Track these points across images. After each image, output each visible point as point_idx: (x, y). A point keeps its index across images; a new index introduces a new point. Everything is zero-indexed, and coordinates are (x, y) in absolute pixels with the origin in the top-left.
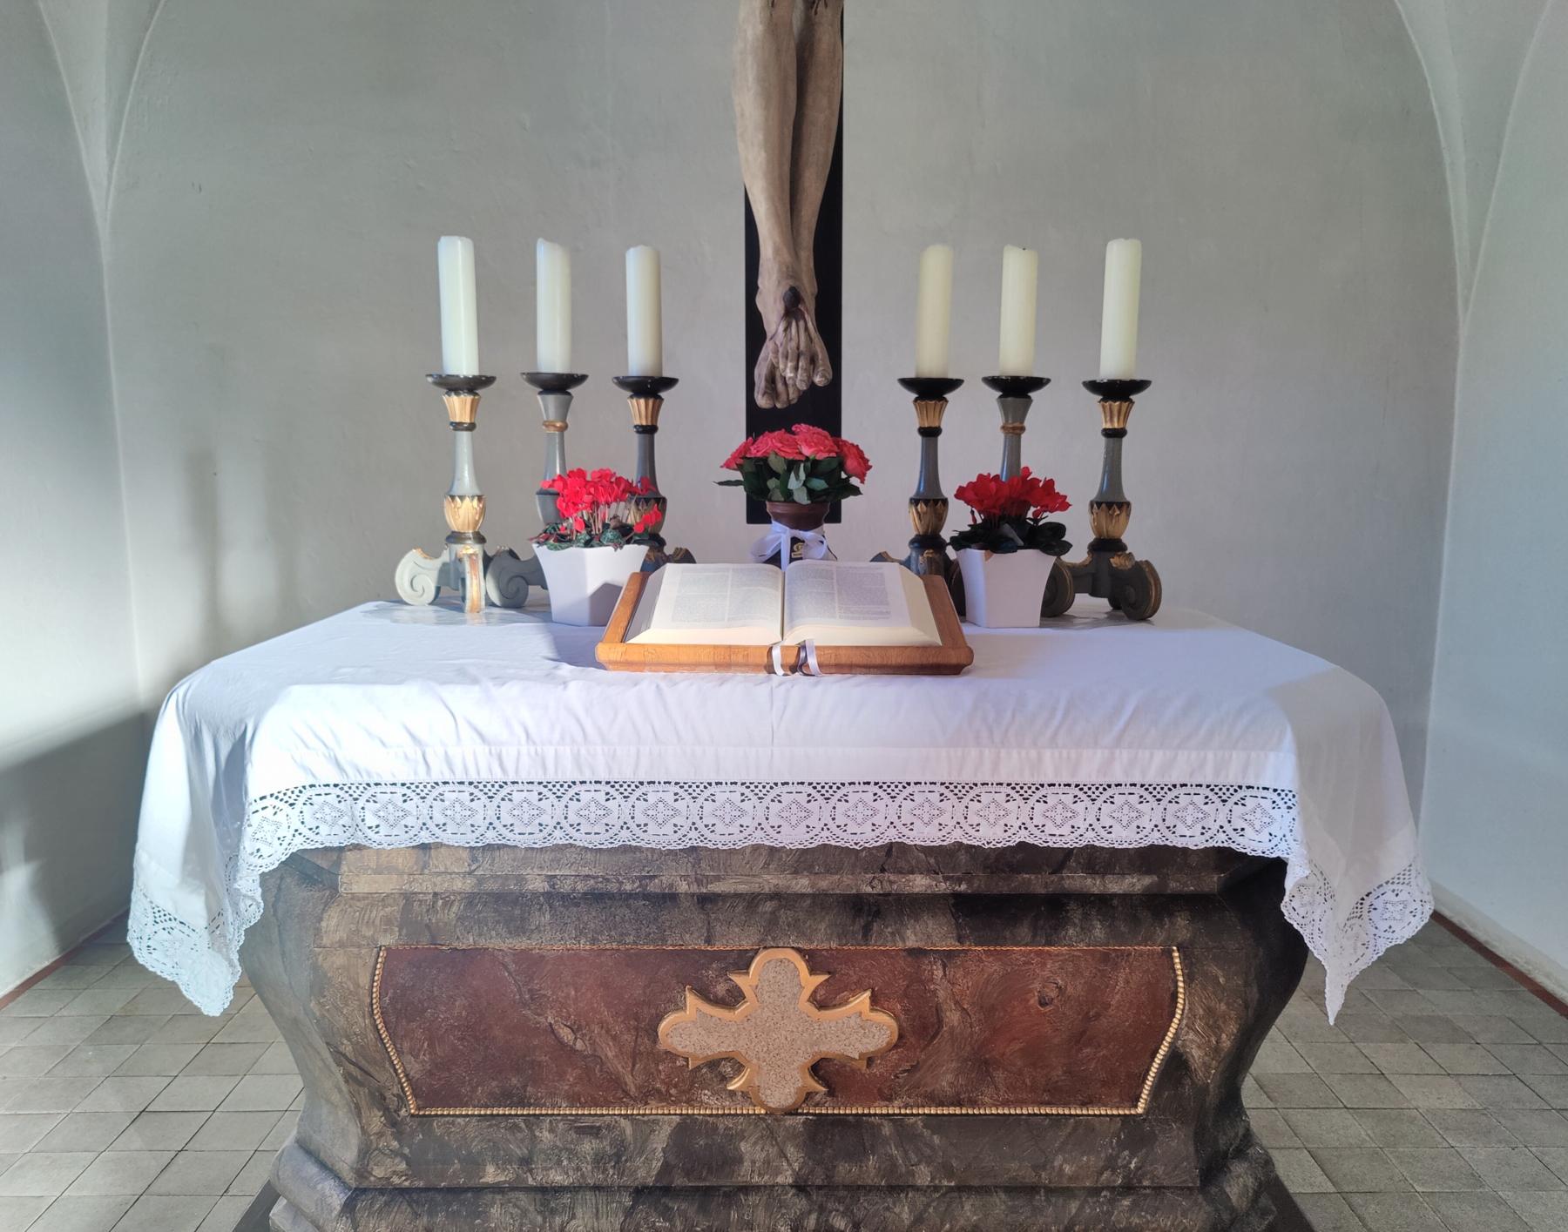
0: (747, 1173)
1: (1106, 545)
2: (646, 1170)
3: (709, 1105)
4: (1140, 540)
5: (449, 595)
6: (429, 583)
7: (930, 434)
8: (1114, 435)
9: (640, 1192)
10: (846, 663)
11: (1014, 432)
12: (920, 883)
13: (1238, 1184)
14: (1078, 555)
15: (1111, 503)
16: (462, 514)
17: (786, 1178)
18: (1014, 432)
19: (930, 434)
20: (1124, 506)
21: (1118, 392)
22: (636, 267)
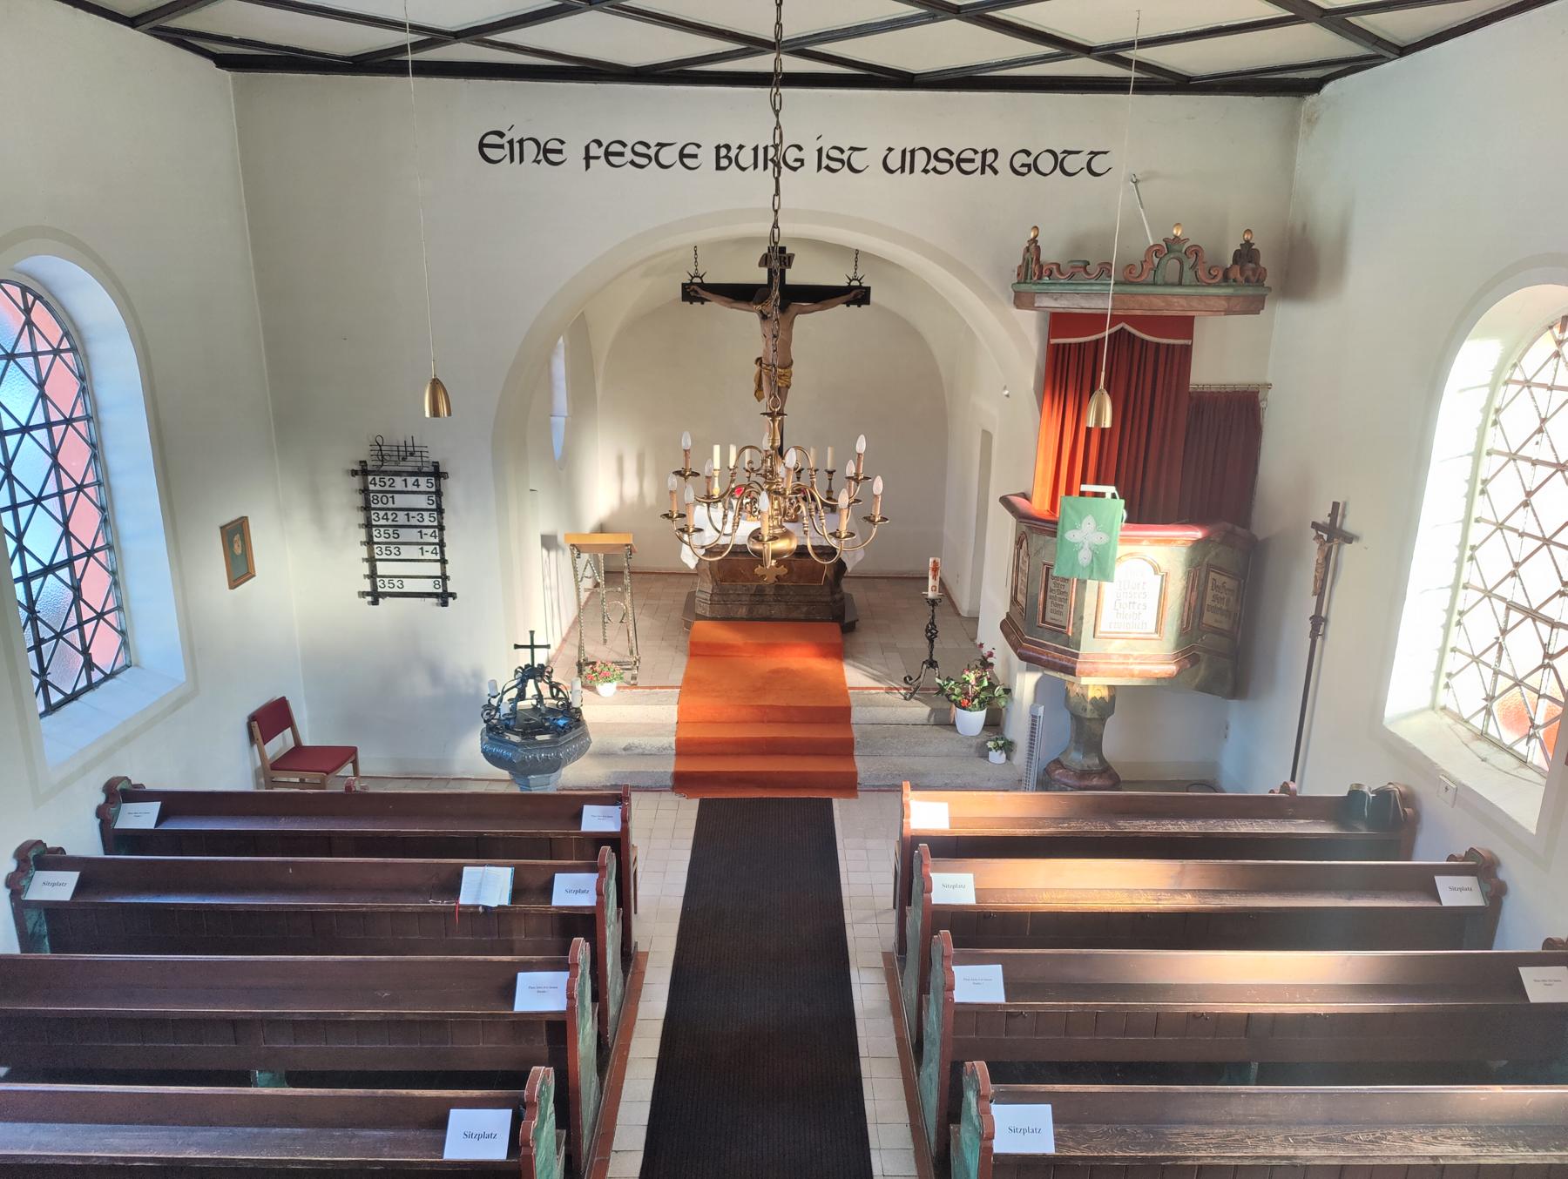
0: (766, 593)
2: (753, 592)
8: (830, 479)
9: (751, 595)
13: (837, 596)
17: (771, 593)
20: (832, 492)
21: (831, 473)
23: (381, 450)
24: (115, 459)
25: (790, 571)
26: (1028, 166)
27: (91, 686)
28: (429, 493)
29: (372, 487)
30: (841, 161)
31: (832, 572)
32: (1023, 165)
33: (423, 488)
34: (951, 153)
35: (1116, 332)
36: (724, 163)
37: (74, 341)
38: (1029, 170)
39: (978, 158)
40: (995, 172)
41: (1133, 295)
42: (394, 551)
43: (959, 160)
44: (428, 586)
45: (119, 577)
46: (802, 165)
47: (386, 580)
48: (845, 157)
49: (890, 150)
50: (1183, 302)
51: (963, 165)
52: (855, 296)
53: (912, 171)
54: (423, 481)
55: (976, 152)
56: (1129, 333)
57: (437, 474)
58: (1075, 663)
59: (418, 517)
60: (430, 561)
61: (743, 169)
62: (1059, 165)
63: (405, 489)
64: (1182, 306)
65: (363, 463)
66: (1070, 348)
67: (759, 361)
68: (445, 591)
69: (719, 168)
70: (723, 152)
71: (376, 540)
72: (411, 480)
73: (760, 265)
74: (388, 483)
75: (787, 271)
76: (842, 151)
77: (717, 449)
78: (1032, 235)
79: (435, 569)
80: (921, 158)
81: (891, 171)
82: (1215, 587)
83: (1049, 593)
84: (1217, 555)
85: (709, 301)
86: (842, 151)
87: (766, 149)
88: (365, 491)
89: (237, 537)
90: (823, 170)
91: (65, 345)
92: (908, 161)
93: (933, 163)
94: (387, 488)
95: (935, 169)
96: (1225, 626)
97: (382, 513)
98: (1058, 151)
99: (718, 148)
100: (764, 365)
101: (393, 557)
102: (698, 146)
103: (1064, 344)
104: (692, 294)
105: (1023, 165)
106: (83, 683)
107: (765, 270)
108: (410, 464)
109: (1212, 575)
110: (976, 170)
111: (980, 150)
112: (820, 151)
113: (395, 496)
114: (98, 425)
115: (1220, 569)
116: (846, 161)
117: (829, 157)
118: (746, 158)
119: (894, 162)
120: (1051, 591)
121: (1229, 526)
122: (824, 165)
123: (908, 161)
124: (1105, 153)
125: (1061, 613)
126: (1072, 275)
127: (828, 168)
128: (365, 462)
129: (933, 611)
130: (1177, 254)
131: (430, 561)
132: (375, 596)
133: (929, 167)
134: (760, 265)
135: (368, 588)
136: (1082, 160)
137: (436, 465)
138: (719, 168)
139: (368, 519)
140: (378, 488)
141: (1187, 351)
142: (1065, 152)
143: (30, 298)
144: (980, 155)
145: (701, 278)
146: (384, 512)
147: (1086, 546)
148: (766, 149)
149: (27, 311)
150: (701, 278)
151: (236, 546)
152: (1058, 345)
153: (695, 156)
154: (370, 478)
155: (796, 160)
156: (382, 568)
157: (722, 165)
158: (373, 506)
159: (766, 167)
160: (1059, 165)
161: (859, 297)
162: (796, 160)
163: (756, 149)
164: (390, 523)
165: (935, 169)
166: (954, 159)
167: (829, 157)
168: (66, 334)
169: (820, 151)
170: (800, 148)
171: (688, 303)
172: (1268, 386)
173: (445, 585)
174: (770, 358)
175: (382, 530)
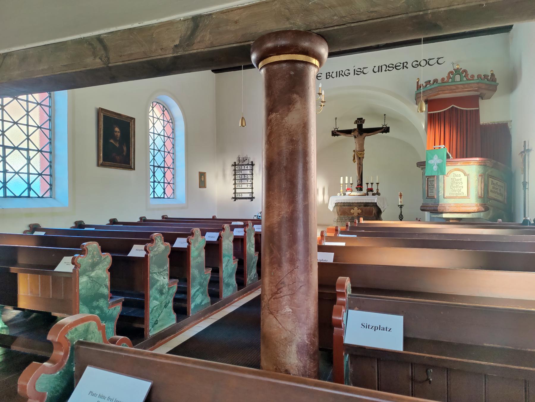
1: (377, 192)
2: (350, 219)
3: (353, 216)
4: (379, 192)
5: (341, 195)
6: (339, 195)
7: (367, 186)
8: (378, 186)
10: (359, 195)
11: (372, 186)
12: (362, 205)
14: (375, 192)
15: (378, 190)
16: (341, 190)
18: (372, 186)
19: (367, 186)
20: (378, 190)
21: (378, 184)
22: (351, 178)
23: (239, 159)
24: (177, 148)
25: (362, 211)
26: (418, 65)
27: (164, 198)
28: (250, 170)
29: (236, 169)
30: (361, 72)
31: (376, 212)
32: (416, 65)
33: (249, 168)
34: (393, 65)
35: (451, 108)
36: (328, 77)
37: (172, 121)
38: (418, 66)
39: (402, 65)
40: (407, 68)
41: (444, 86)
42: (241, 186)
43: (396, 66)
44: (248, 195)
45: (174, 176)
46: (350, 74)
47: (238, 194)
48: (362, 71)
49: (375, 67)
50: (462, 86)
51: (397, 68)
52: (384, 130)
53: (381, 71)
54: (249, 166)
55: (401, 63)
56: (456, 108)
57: (253, 165)
58: (437, 207)
59: (247, 176)
60: (249, 188)
61: (333, 78)
62: (427, 63)
63: (244, 169)
64: (462, 88)
65: (235, 163)
66: (433, 115)
67: (354, 151)
68: (252, 197)
69: (327, 78)
70: (328, 74)
71: (236, 183)
72: (246, 166)
73: (354, 123)
74: (240, 168)
75: (363, 124)
76: (361, 69)
77: (342, 178)
78: (417, 81)
79: (250, 191)
80: (384, 68)
81: (375, 72)
82: (493, 183)
83: (429, 187)
84: (491, 172)
85: (340, 135)
86: (361, 69)
87: (339, 72)
88: (235, 170)
89: (203, 176)
90: (356, 75)
91: (170, 121)
92: (380, 69)
93: (388, 68)
94: (240, 169)
95: (388, 70)
96: (500, 198)
97: (238, 176)
98: (427, 60)
99: (327, 74)
100: (355, 152)
101: (240, 187)
102: (321, 74)
103: (433, 113)
104: (334, 133)
105: (416, 65)
106: (162, 196)
107: (356, 125)
108: (246, 163)
109: (490, 179)
110: (400, 69)
111: (402, 63)
112: (355, 70)
113: (242, 171)
114: (175, 140)
115: (493, 177)
116: (362, 71)
117: (357, 71)
118: (334, 75)
119: (376, 70)
120: (429, 186)
121: (495, 161)
122: (356, 73)
123: (380, 69)
124: (443, 58)
125: (433, 192)
126: (426, 85)
127: (357, 74)
128: (235, 162)
129: (401, 210)
130: (458, 73)
131: (249, 188)
132: (235, 199)
133: (387, 70)
134: (354, 123)
135: (234, 197)
136: (435, 60)
137: (252, 162)
138: (327, 78)
139: (235, 177)
140: (238, 169)
141: (477, 111)
142: (429, 59)
143: (164, 109)
144: (402, 64)
145: (337, 129)
146: (239, 176)
147: (435, 164)
148: (339, 72)
149: (163, 111)
150: (337, 129)
151: (202, 178)
152: (431, 114)
153: (321, 76)
154: (236, 166)
155: (348, 73)
156: (237, 191)
157: (328, 77)
158: (236, 174)
159: (339, 76)
160: (427, 63)
161: (386, 130)
162: (348, 73)
163: (337, 72)
164: (240, 178)
165: (388, 70)
166: (394, 66)
167: (357, 71)
168: (171, 119)
169: (355, 70)
170: (349, 70)
171: (334, 137)
172: (511, 121)
173: (252, 195)
174: (358, 150)
175: (238, 180)
